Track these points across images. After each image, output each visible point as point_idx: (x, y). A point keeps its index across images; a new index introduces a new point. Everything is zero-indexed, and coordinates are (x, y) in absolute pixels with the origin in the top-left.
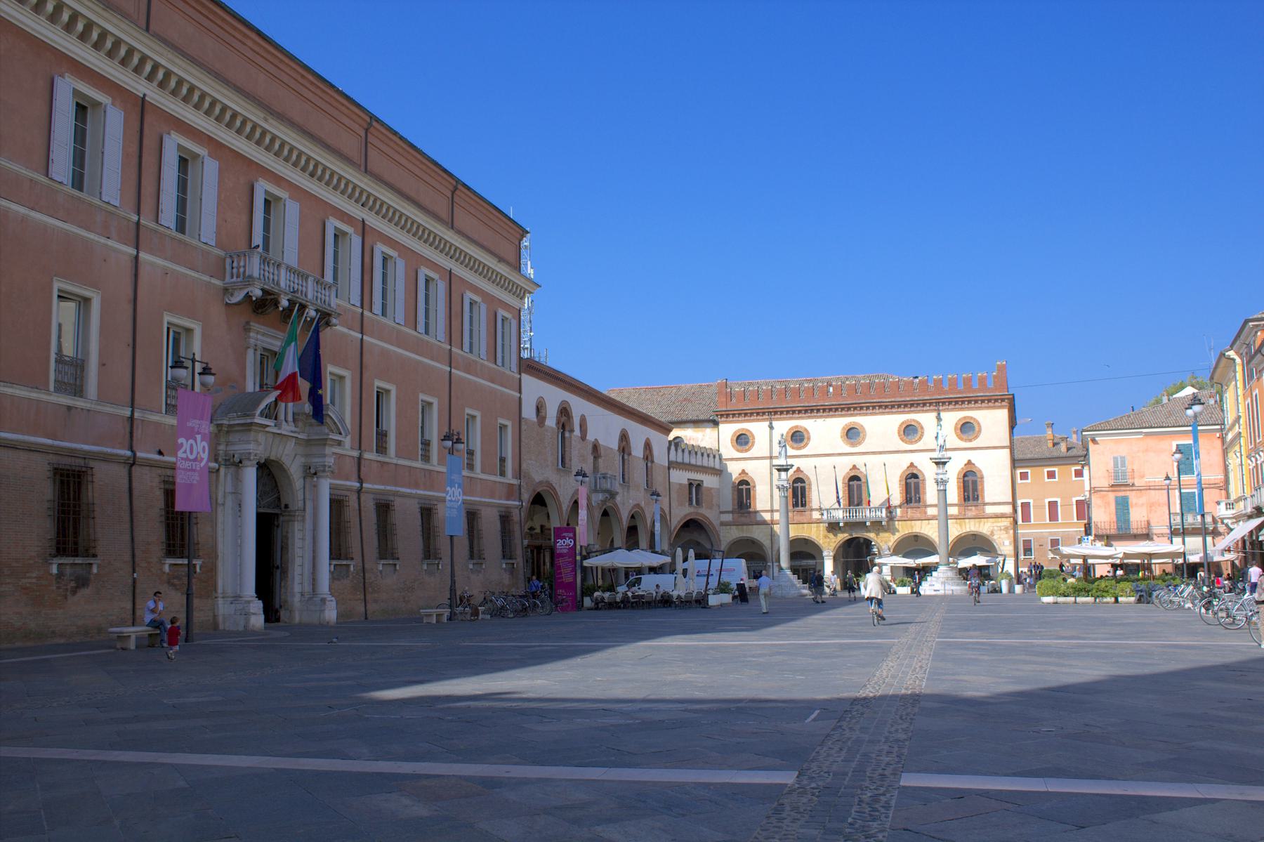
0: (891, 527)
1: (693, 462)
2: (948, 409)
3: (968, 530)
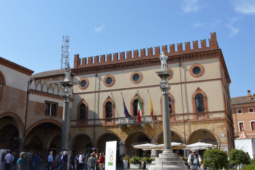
0: (156, 128)
1: (50, 92)
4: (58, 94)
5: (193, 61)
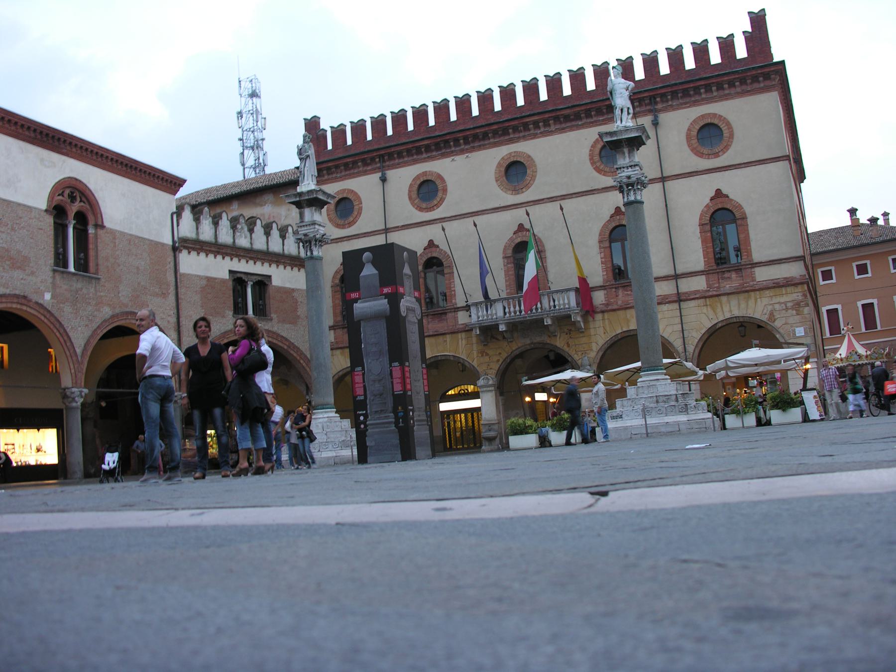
1: (243, 241)
2: (671, 106)
3: (728, 315)
4: (268, 249)
5: (698, 105)
